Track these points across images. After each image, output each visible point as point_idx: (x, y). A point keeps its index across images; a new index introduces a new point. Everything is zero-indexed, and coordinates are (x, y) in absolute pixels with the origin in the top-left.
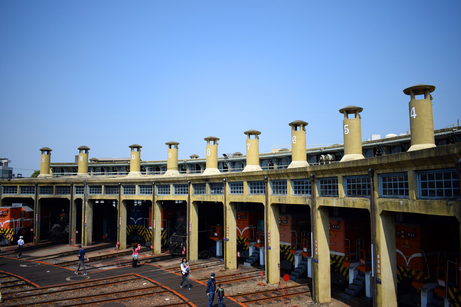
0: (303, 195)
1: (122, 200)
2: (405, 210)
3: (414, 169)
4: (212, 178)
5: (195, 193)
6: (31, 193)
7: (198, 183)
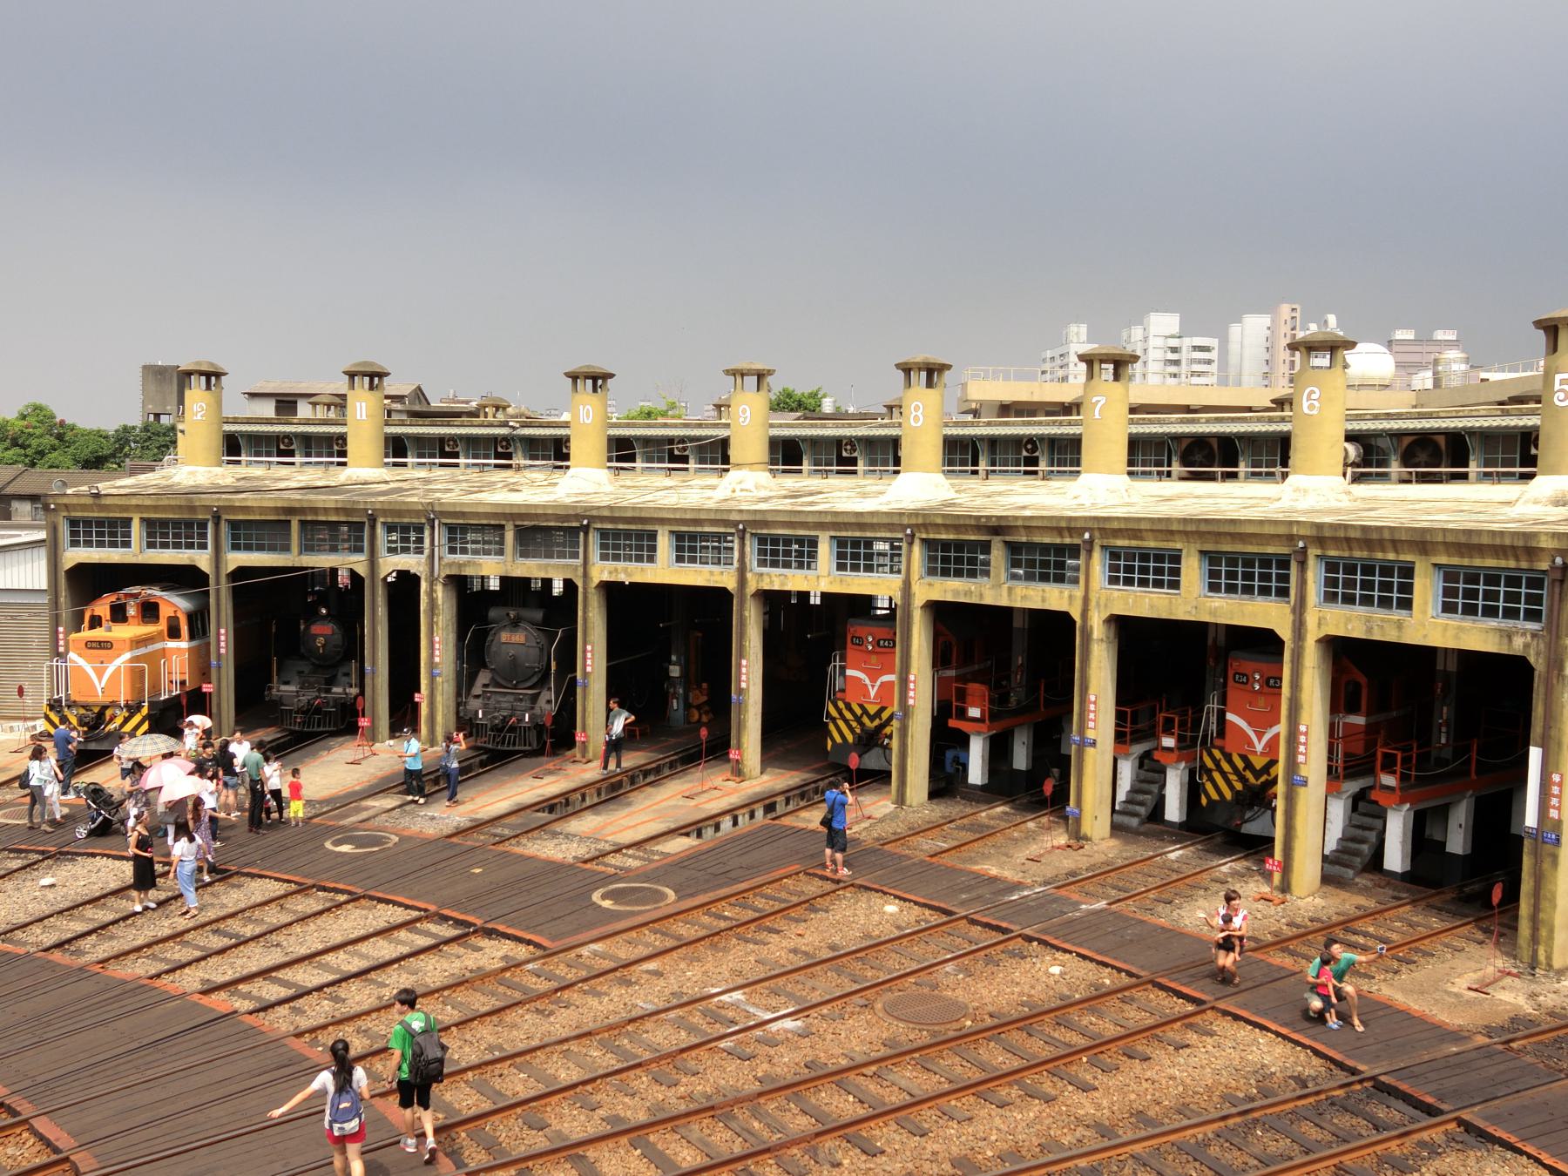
0: (1493, 623)
1: (596, 581)
4: (1026, 527)
5: (931, 572)
6: (190, 546)
7: (951, 537)
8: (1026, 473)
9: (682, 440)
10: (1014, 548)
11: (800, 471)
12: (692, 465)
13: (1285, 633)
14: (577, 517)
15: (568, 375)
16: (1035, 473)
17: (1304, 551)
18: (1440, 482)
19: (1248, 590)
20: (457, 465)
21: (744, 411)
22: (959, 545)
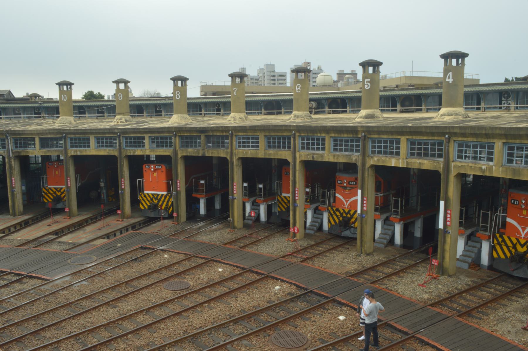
0: (347, 153)
1: (69, 155)
2: (487, 174)
3: (504, 141)
5: (183, 146)
8: (217, 114)
9: (102, 106)
10: (208, 137)
11: (143, 116)
12: (106, 115)
13: (290, 160)
14: (62, 133)
15: (57, 84)
16: (219, 114)
17: (295, 134)
18: (339, 113)
19: (279, 147)
20: (20, 117)
21: (120, 95)
22: (191, 137)
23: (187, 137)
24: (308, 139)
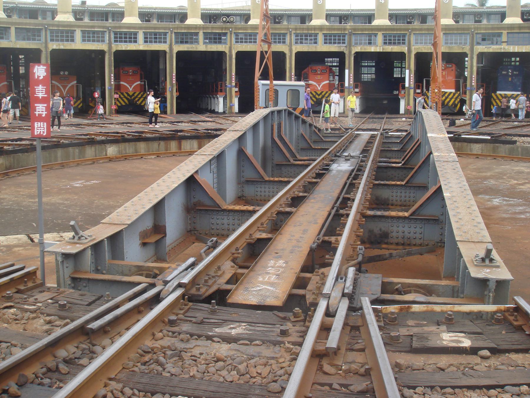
0: (336, 45)
1: (50, 49)
13: (287, 52)
23: (183, 34)
24: (301, 36)
